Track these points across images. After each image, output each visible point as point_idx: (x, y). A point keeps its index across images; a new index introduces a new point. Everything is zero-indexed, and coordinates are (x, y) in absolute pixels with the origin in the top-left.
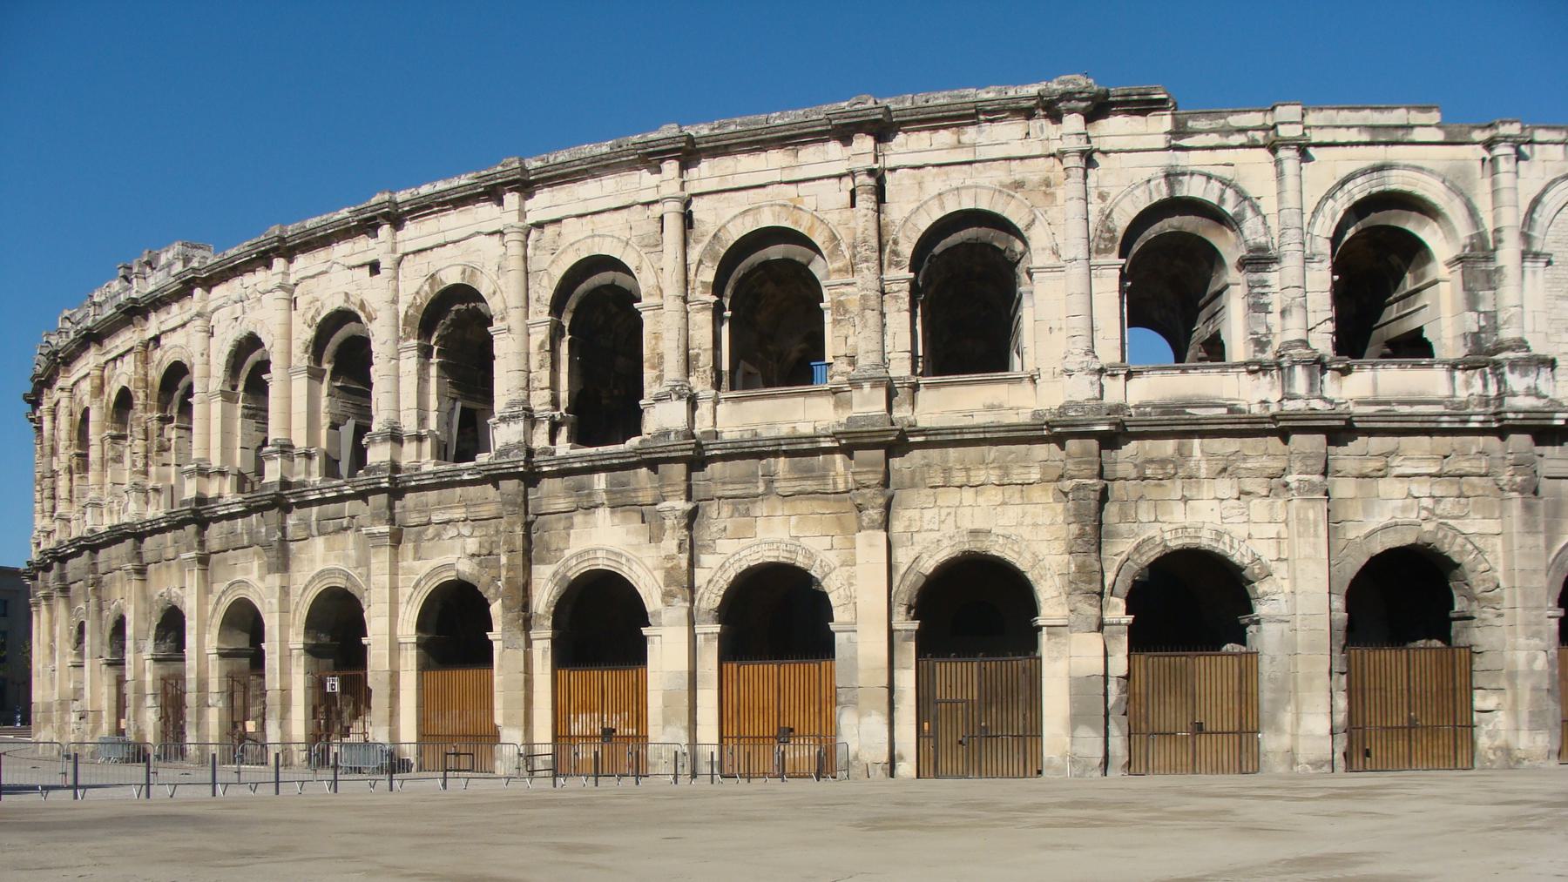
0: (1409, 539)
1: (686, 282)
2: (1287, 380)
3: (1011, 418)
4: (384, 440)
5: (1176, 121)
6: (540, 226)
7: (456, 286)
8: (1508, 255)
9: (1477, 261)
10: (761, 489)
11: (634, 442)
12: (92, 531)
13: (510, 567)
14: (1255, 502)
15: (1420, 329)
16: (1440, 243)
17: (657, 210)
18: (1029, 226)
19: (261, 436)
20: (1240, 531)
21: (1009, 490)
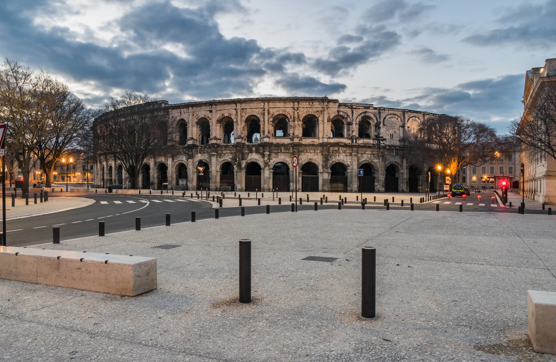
6: (243, 109)
8: (381, 125)
9: (377, 126)
16: (373, 123)
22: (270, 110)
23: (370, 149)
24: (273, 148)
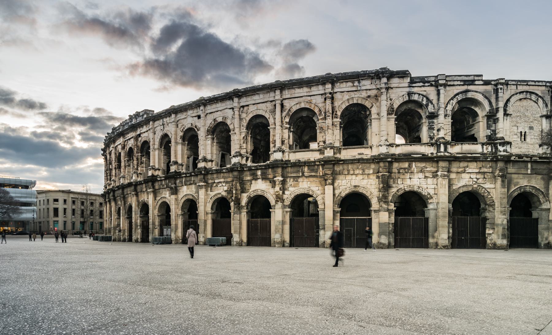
0: (470, 189)
1: (282, 122)
2: (439, 147)
3: (365, 157)
4: (203, 161)
5: (411, 80)
6: (243, 107)
7: (221, 122)
10: (301, 175)
11: (268, 162)
12: (122, 184)
13: (236, 194)
14: (429, 179)
15: (474, 134)
17: (274, 103)
18: (371, 108)
19: (168, 160)
20: (425, 186)
21: (364, 176)
22: (286, 103)
23: (475, 164)
24: (289, 169)
